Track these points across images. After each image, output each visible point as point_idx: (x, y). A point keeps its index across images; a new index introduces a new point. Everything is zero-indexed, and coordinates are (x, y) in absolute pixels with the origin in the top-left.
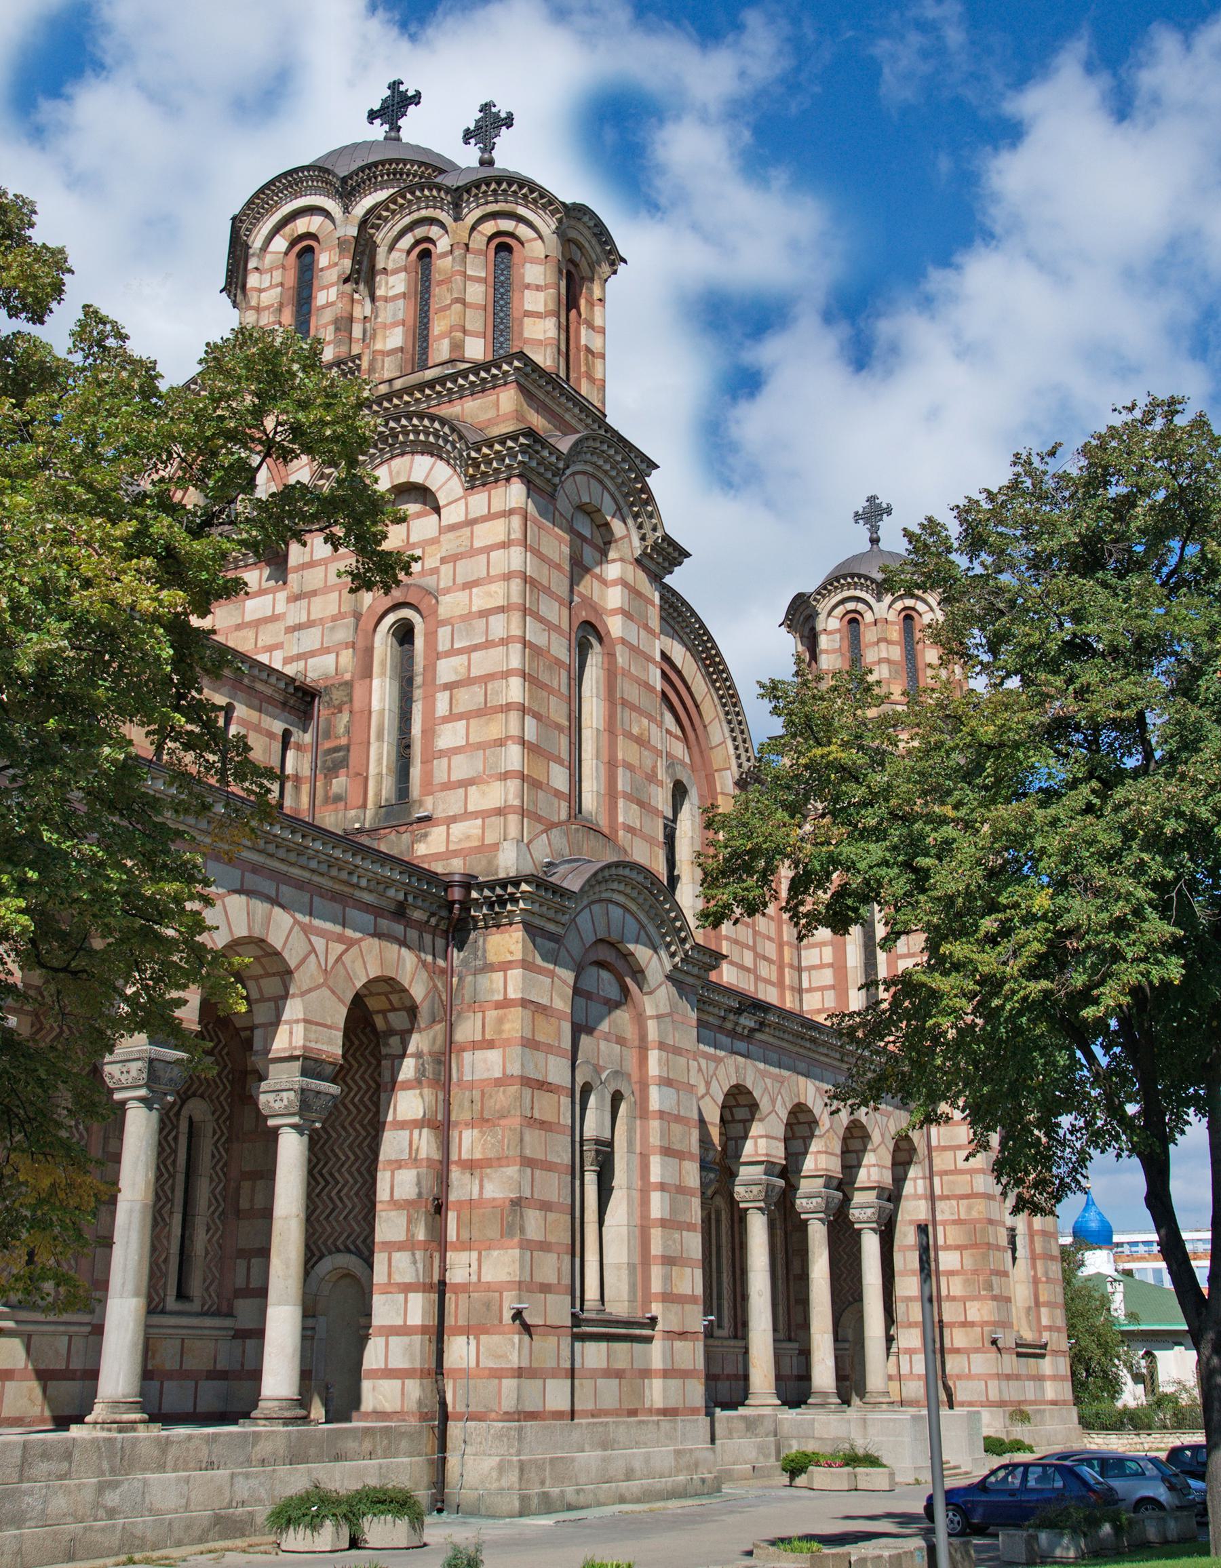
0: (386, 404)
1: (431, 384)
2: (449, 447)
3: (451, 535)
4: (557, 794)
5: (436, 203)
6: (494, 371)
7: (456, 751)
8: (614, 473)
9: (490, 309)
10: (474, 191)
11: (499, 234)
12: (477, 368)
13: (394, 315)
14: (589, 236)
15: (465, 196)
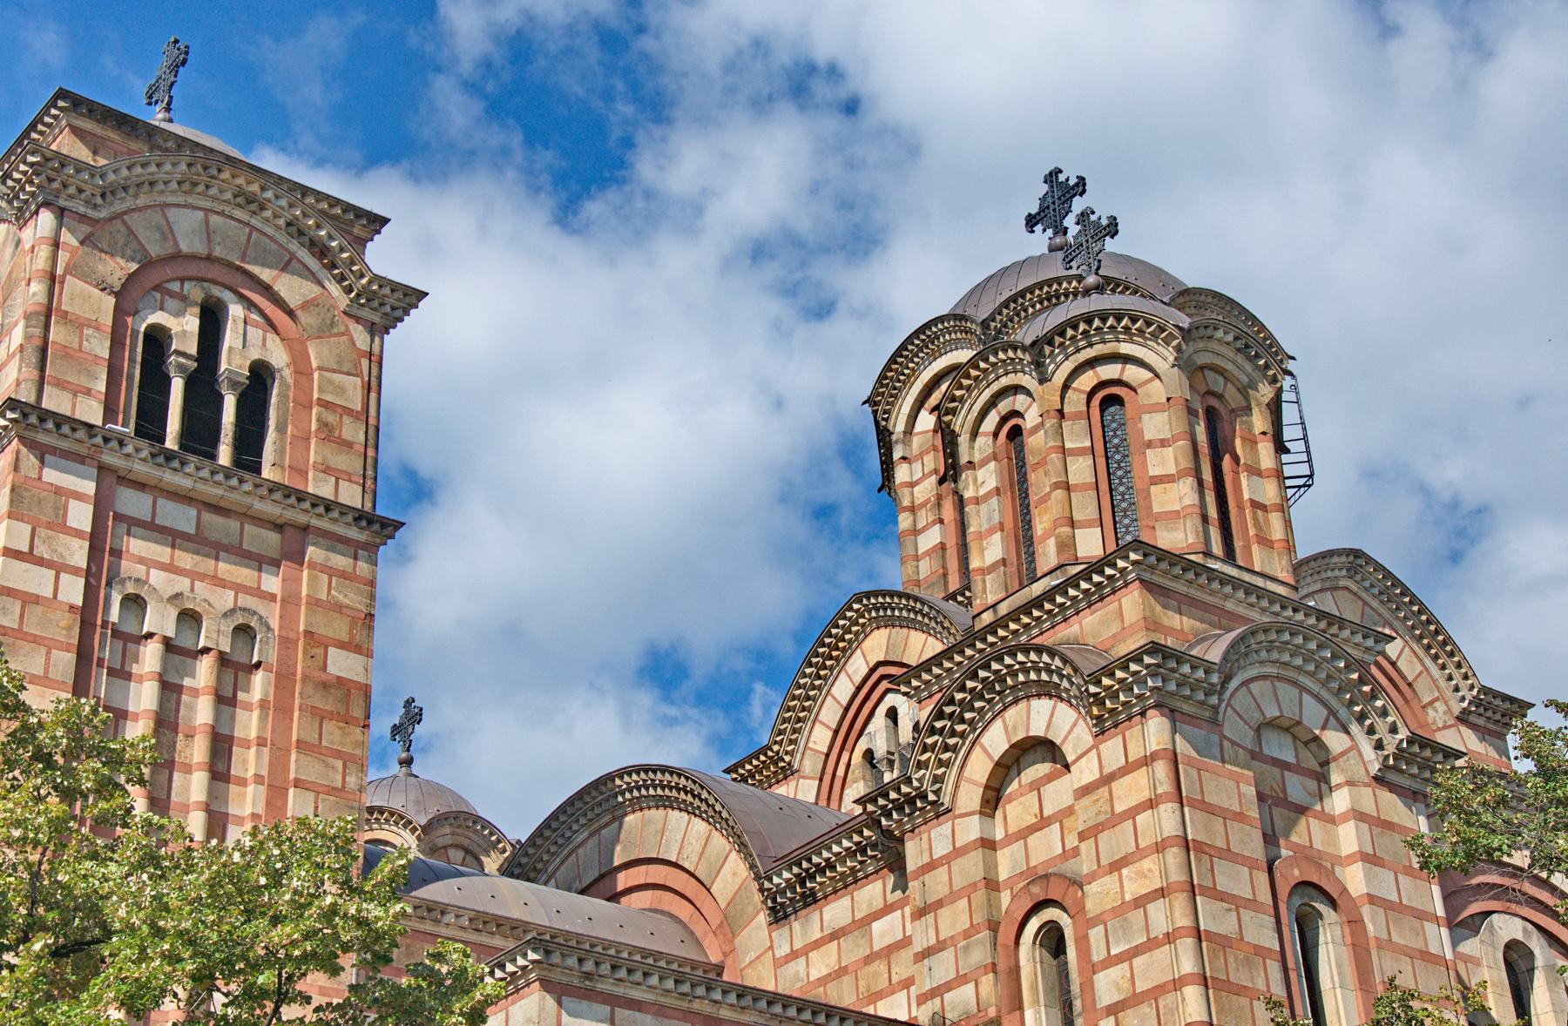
0: (991, 639)
1: (1037, 603)
2: (1065, 684)
3: (1086, 801)
5: (1013, 366)
6: (1109, 571)
8: (1311, 667)
9: (1104, 486)
10: (1058, 340)
12: (1097, 567)
13: (989, 519)
14: (1231, 355)
15: (1047, 349)
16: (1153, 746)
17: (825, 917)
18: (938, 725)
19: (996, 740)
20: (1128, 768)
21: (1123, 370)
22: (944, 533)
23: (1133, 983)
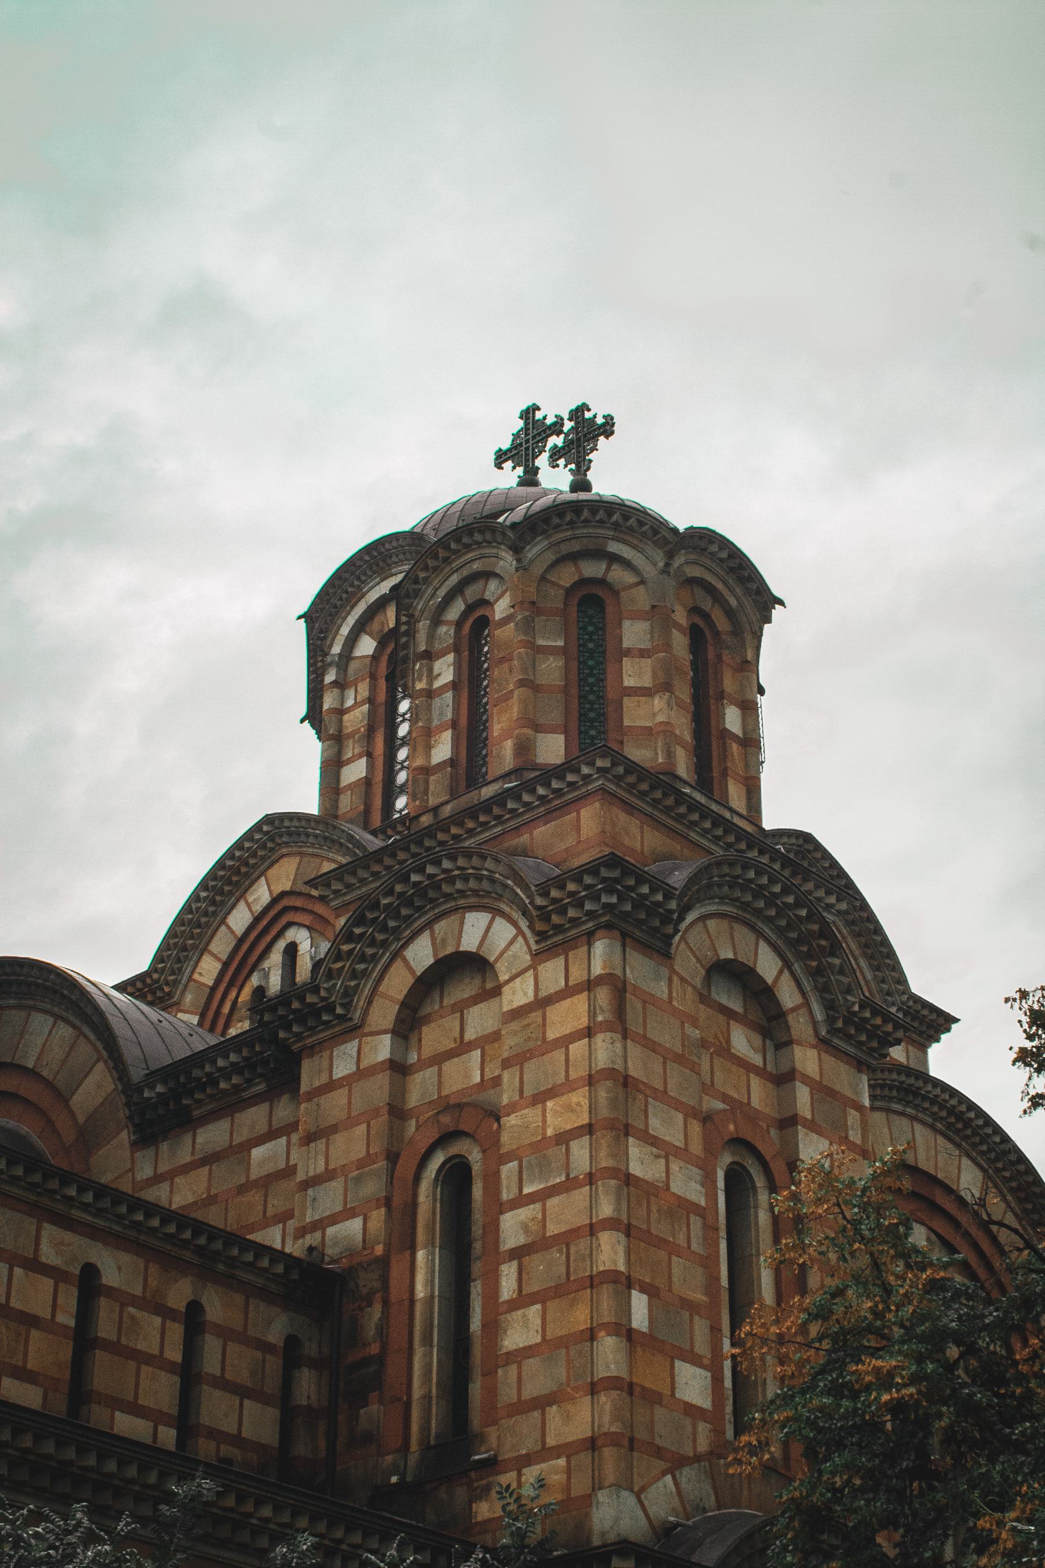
0: (428, 843)
1: (486, 806)
3: (515, 1026)
4: (691, 1410)
7: (528, 1352)
9: (574, 691)
11: (583, 582)
13: (441, 714)
16: (597, 969)
17: (199, 1140)
18: (357, 931)
19: (421, 954)
20: (568, 992)
21: (608, 569)
22: (371, 767)
23: (544, 1226)
